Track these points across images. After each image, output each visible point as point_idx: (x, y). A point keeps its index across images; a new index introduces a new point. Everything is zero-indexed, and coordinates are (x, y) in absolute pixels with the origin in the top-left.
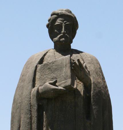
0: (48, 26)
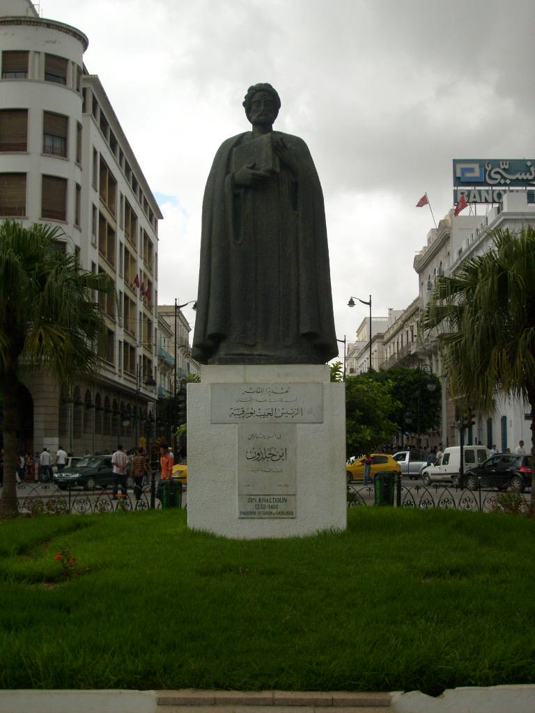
0: (244, 104)
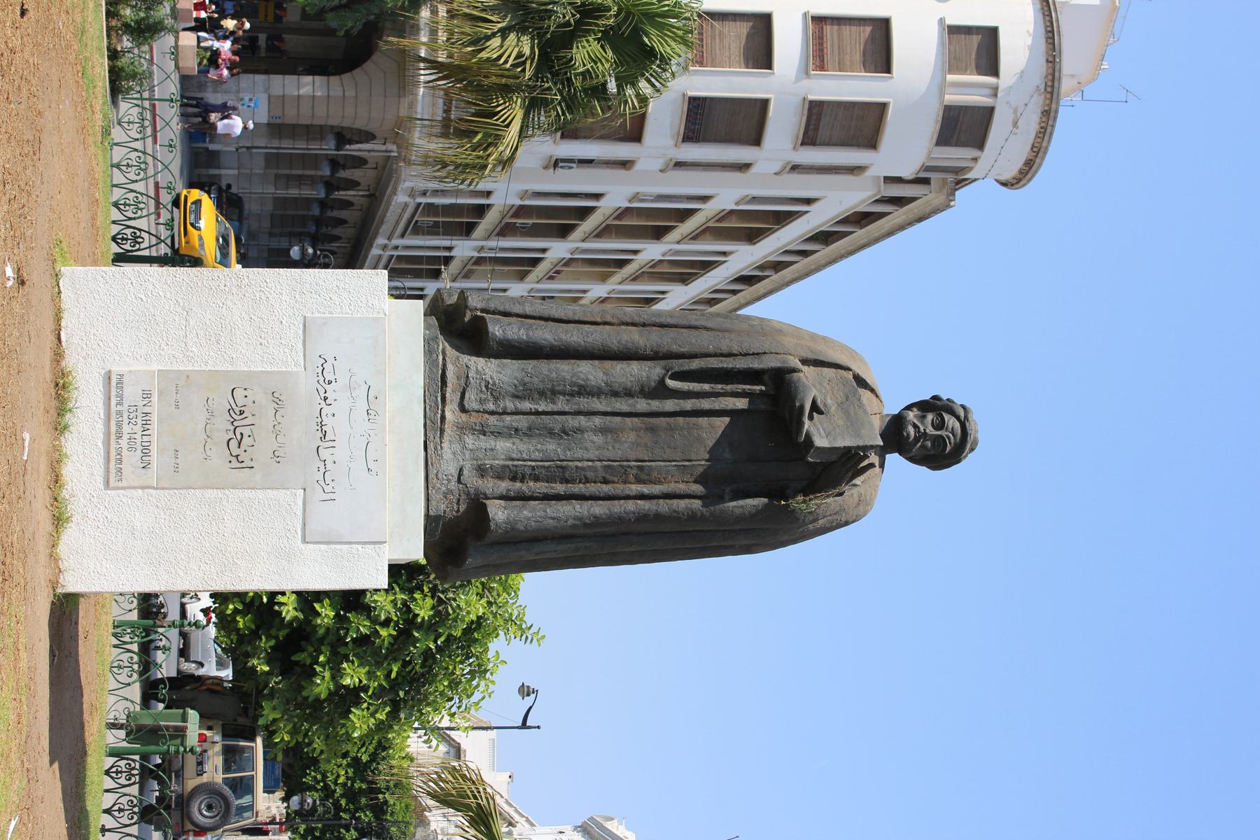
0: (935, 398)
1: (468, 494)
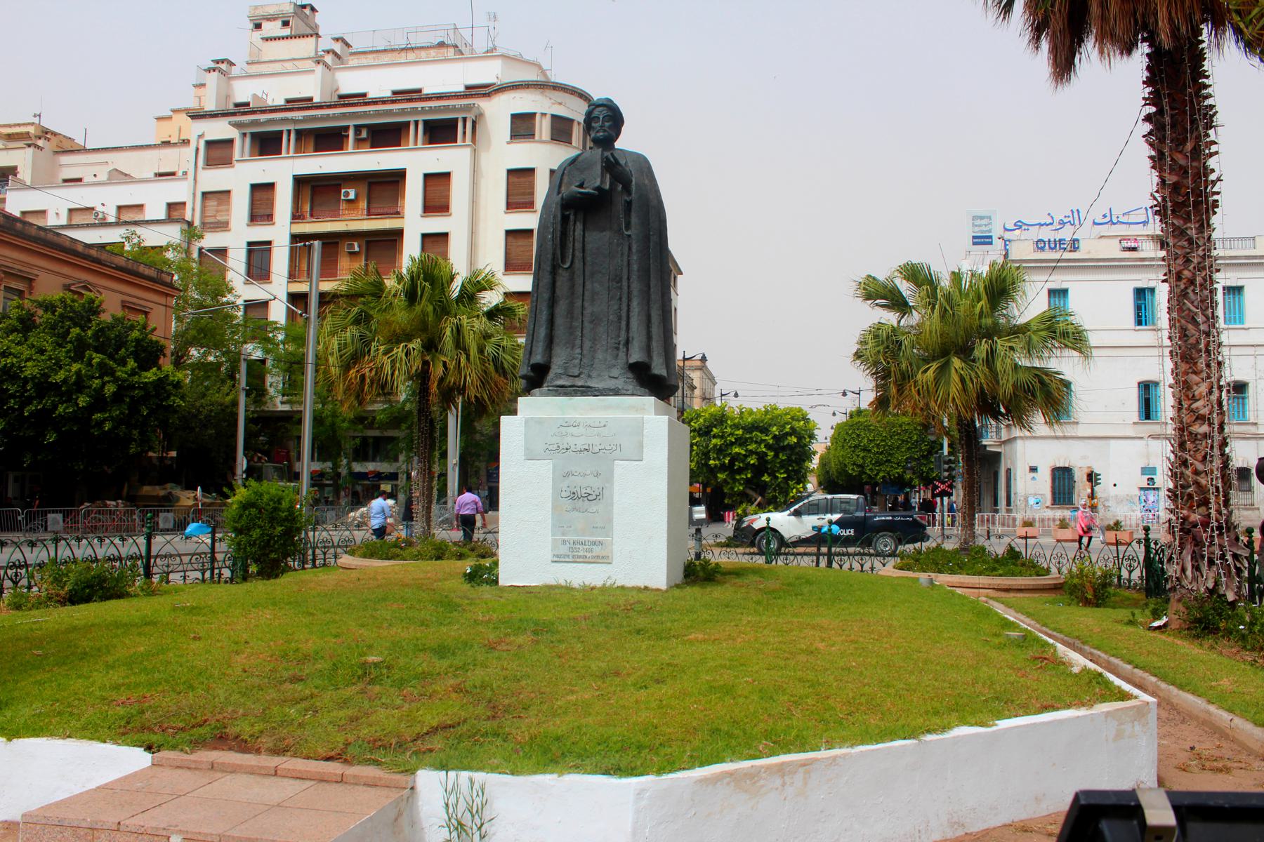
1: (624, 373)
